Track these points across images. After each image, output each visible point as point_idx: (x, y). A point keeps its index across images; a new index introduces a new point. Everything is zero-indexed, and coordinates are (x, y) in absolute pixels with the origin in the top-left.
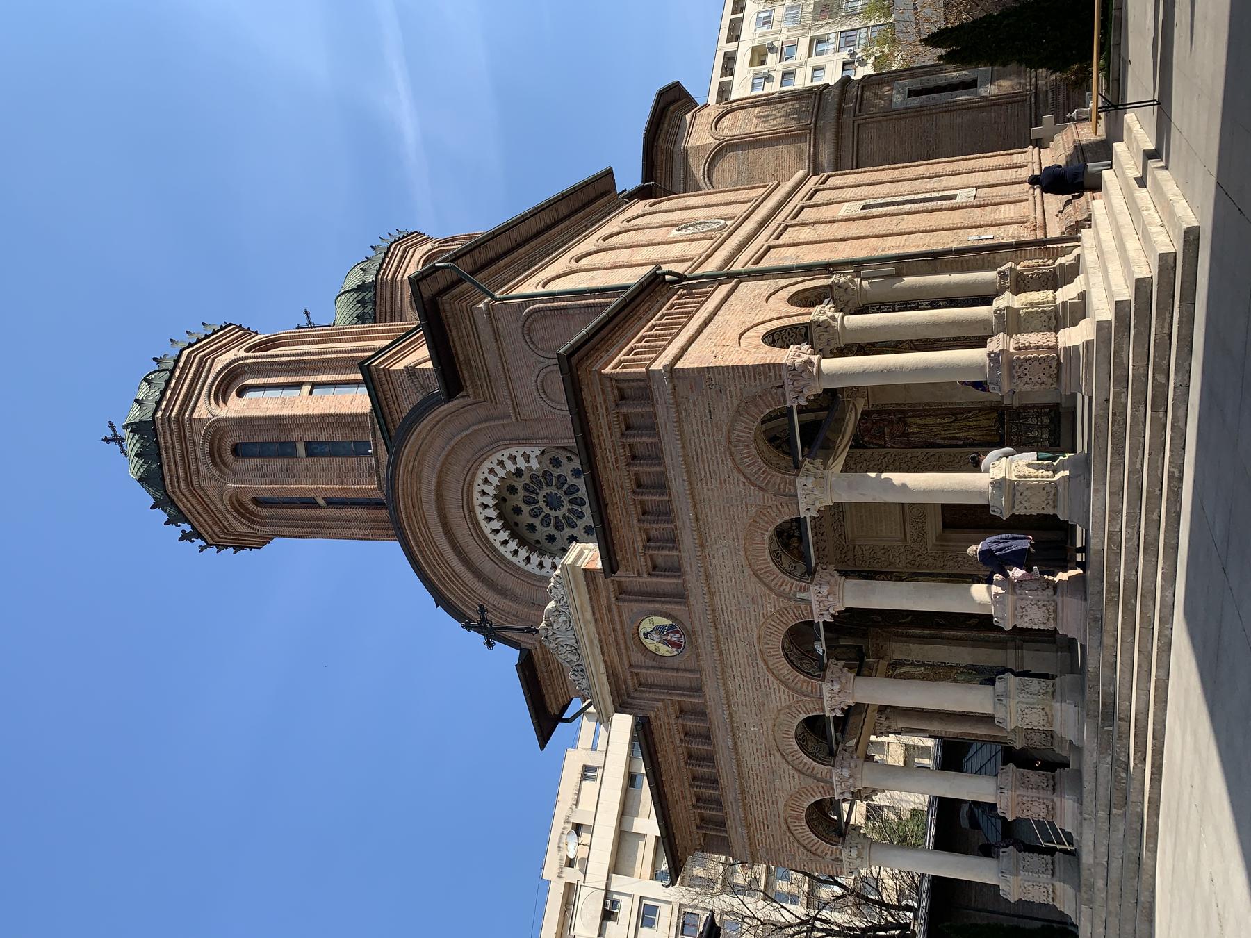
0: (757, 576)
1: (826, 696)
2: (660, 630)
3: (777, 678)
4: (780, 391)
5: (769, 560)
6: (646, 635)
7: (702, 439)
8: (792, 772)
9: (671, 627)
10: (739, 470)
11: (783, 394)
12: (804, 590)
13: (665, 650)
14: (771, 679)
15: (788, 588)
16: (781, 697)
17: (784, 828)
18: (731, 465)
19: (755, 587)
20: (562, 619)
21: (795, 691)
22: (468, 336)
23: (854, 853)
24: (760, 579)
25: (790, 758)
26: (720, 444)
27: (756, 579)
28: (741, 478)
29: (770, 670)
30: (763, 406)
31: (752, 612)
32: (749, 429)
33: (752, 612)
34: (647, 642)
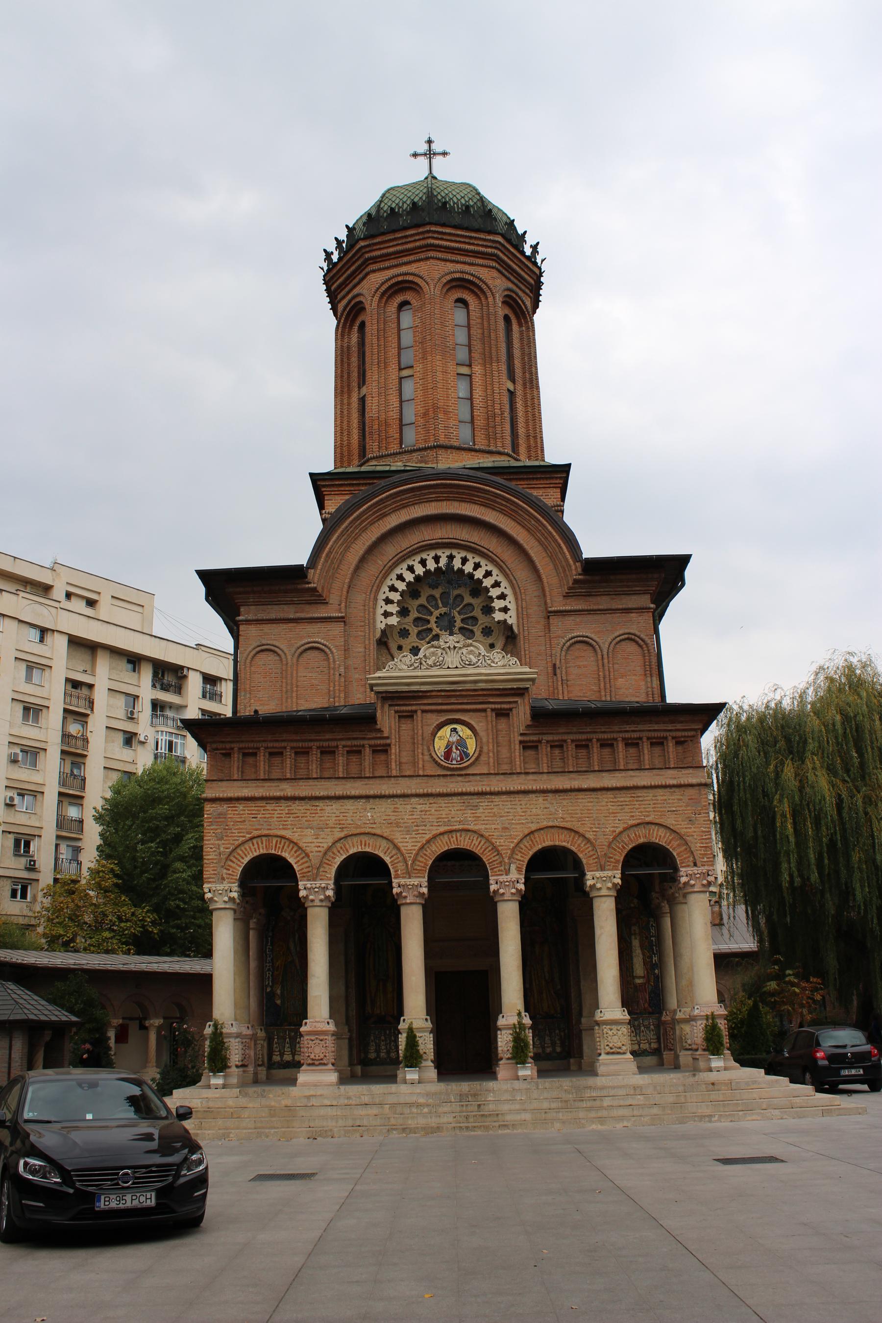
0: (529, 834)
1: (415, 881)
2: (461, 743)
3: (428, 841)
4: (692, 864)
5: (544, 845)
6: (454, 730)
7: (651, 803)
8: (325, 846)
9: (467, 755)
10: (625, 829)
11: (688, 866)
12: (519, 870)
13: (440, 745)
14: (427, 837)
15: (519, 857)
16: (409, 844)
17: (256, 833)
18: (631, 822)
19: (518, 832)
20: (474, 660)
21: (417, 854)
22: (628, 586)
23: (235, 895)
24: (526, 836)
25: (338, 845)
26: (648, 816)
27: (526, 832)
28: (618, 830)
29: (435, 837)
30: (679, 850)
31: (493, 826)
32: (659, 837)
33: (493, 826)
34: (447, 730)
